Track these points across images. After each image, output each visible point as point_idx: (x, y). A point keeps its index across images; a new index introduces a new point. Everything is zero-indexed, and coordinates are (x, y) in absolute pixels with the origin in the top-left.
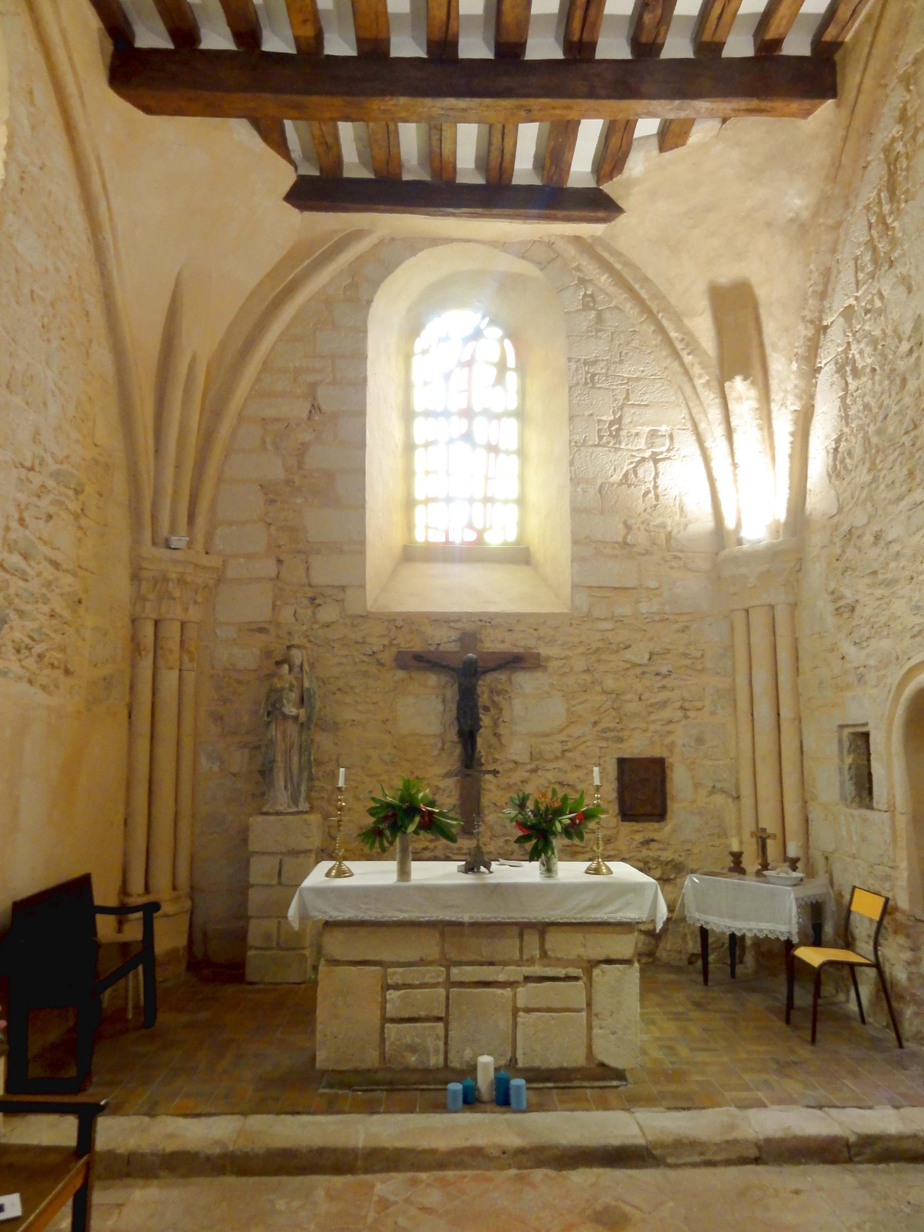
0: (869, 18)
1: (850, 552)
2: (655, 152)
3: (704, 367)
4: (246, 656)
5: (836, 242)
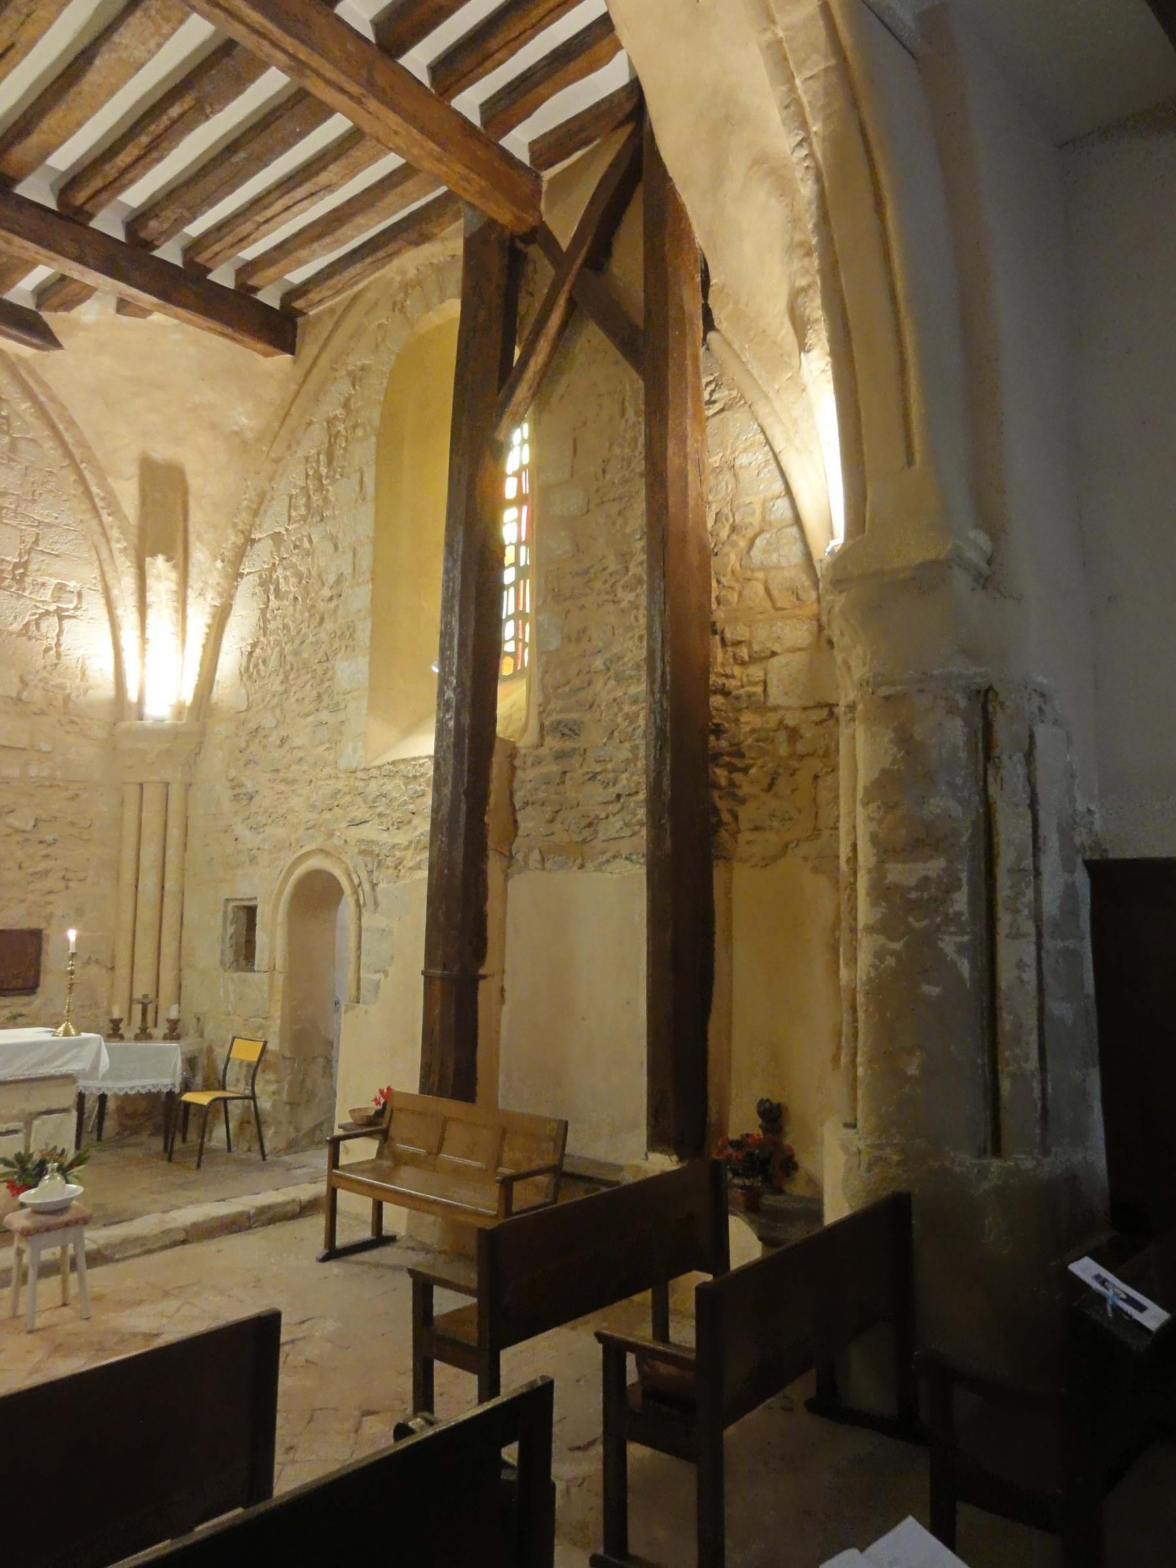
0: (332, 311)
1: (255, 748)
2: (111, 310)
3: (123, 532)
5: (275, 473)
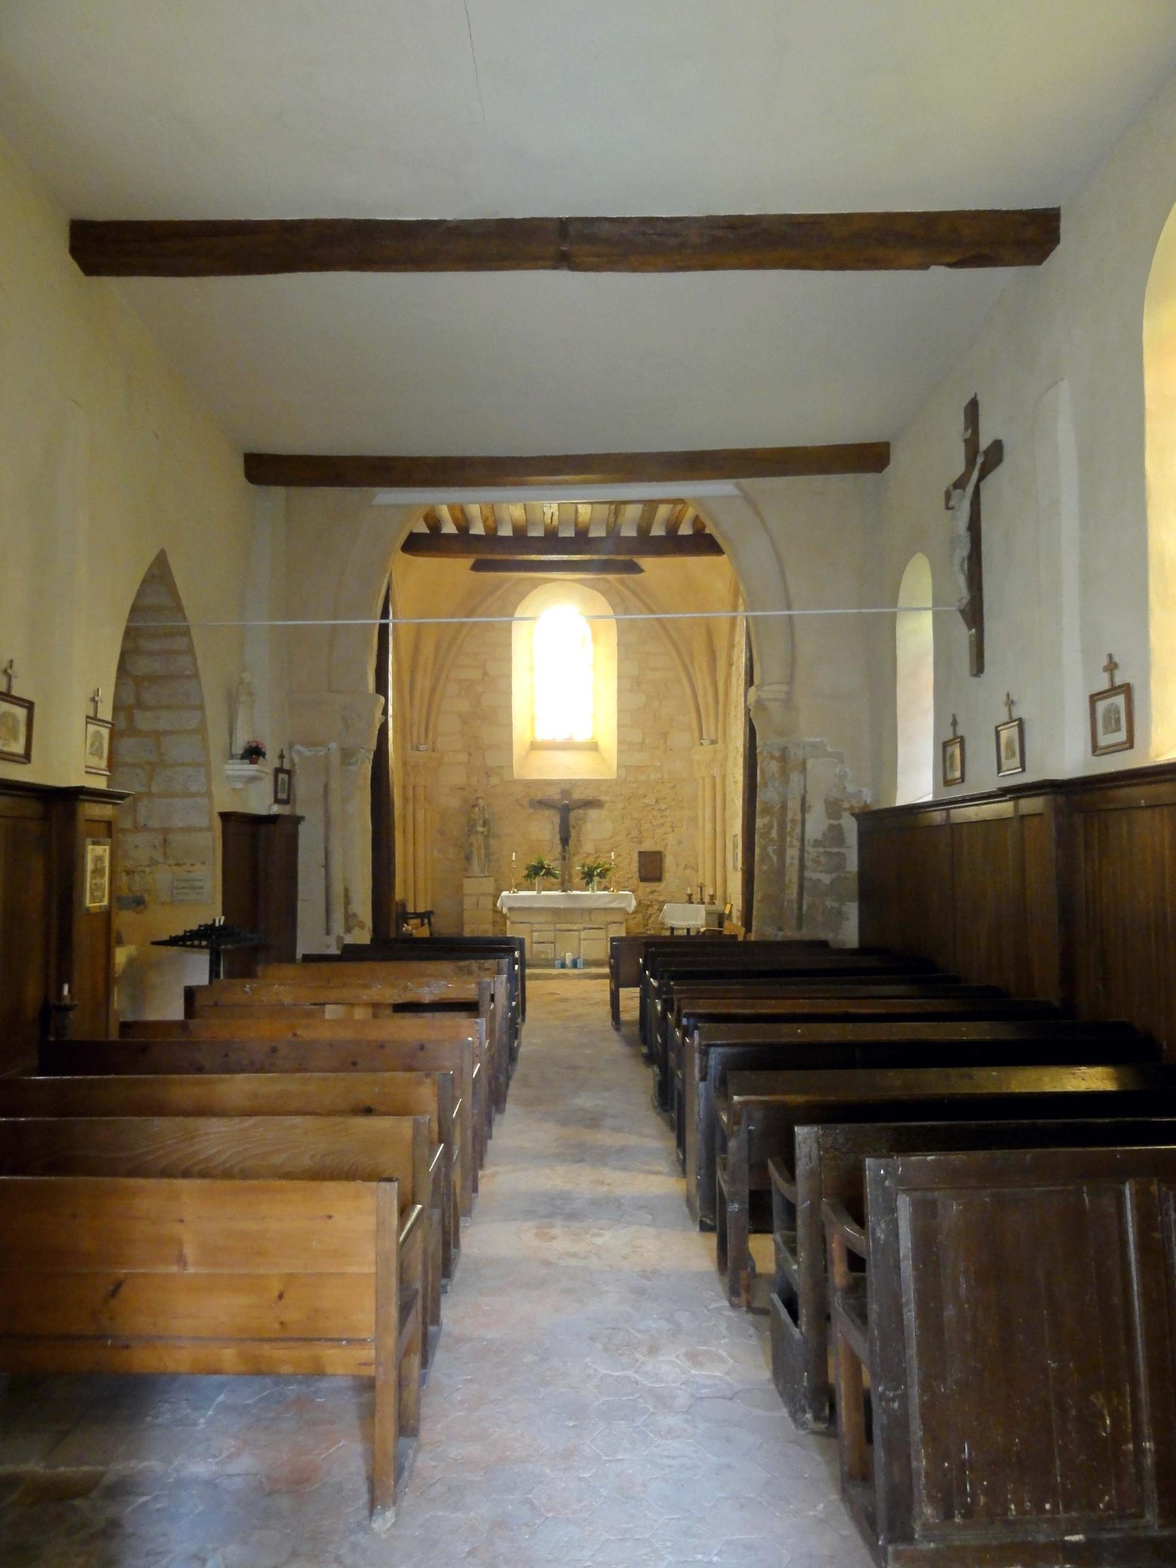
4: (454, 802)
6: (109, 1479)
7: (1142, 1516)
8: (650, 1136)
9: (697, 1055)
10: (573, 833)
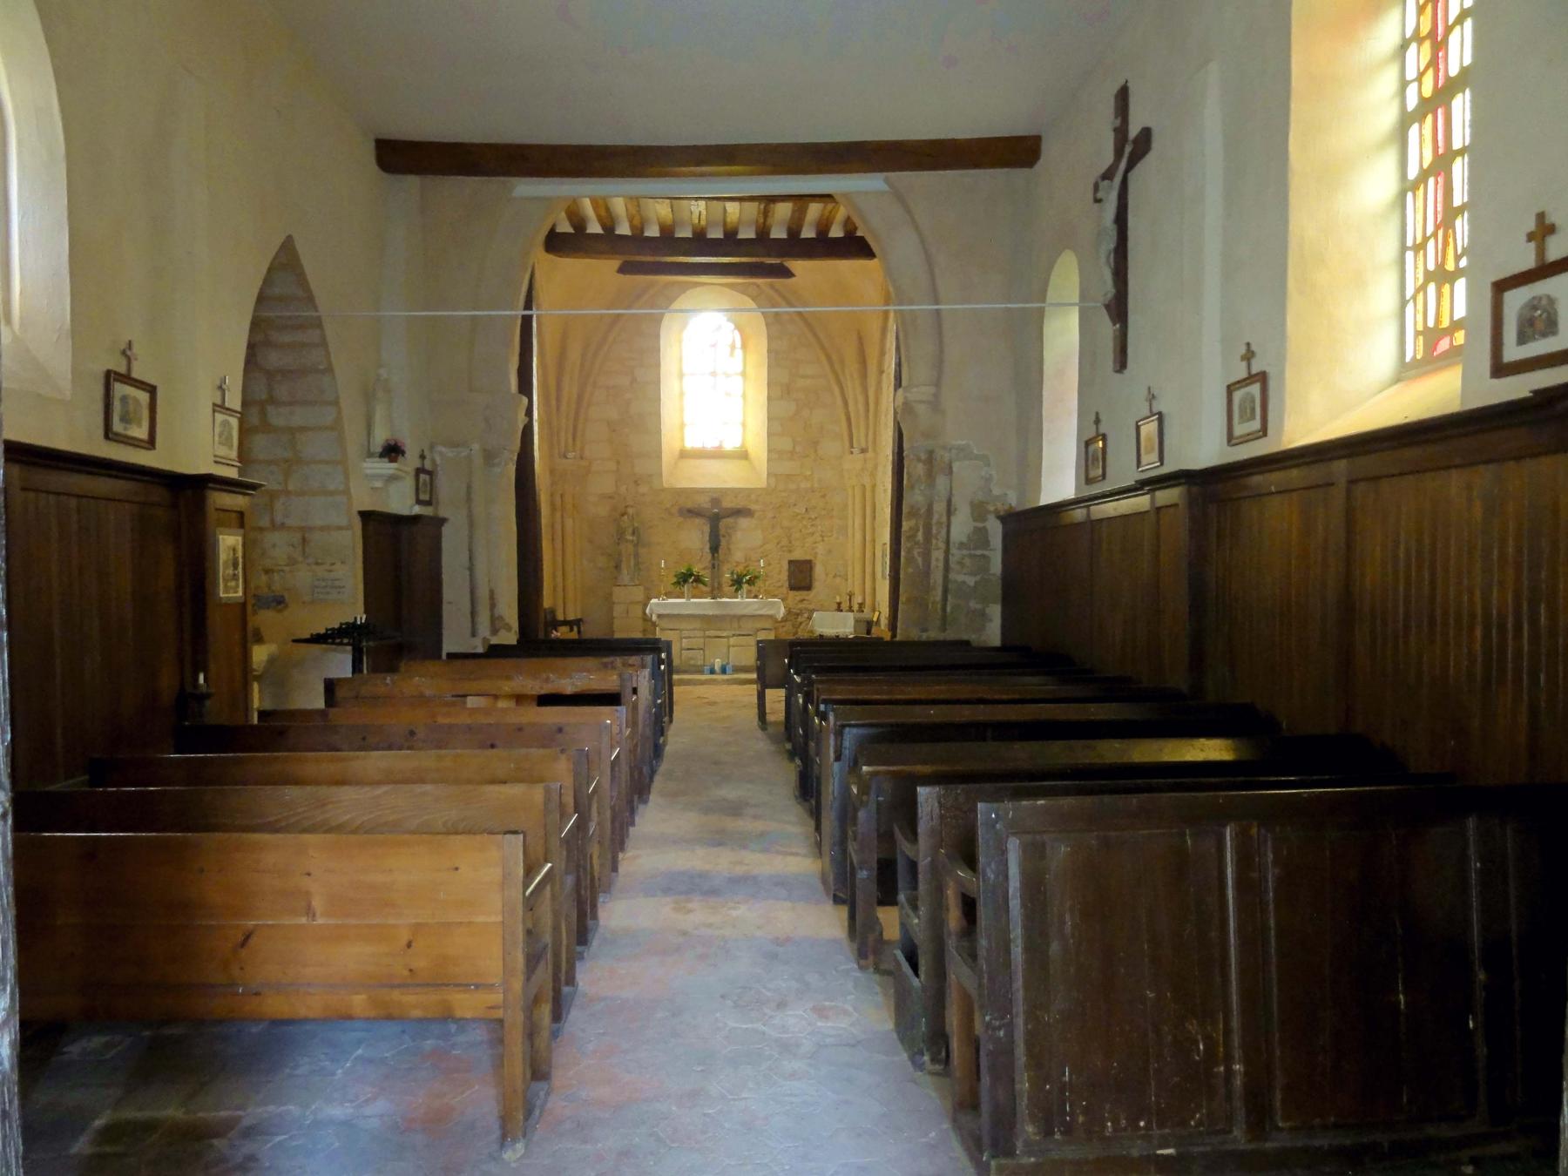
4: (603, 511)
6: (246, 1122)
7: (1230, 1132)
8: (791, 822)
9: (832, 737)
10: (723, 542)
